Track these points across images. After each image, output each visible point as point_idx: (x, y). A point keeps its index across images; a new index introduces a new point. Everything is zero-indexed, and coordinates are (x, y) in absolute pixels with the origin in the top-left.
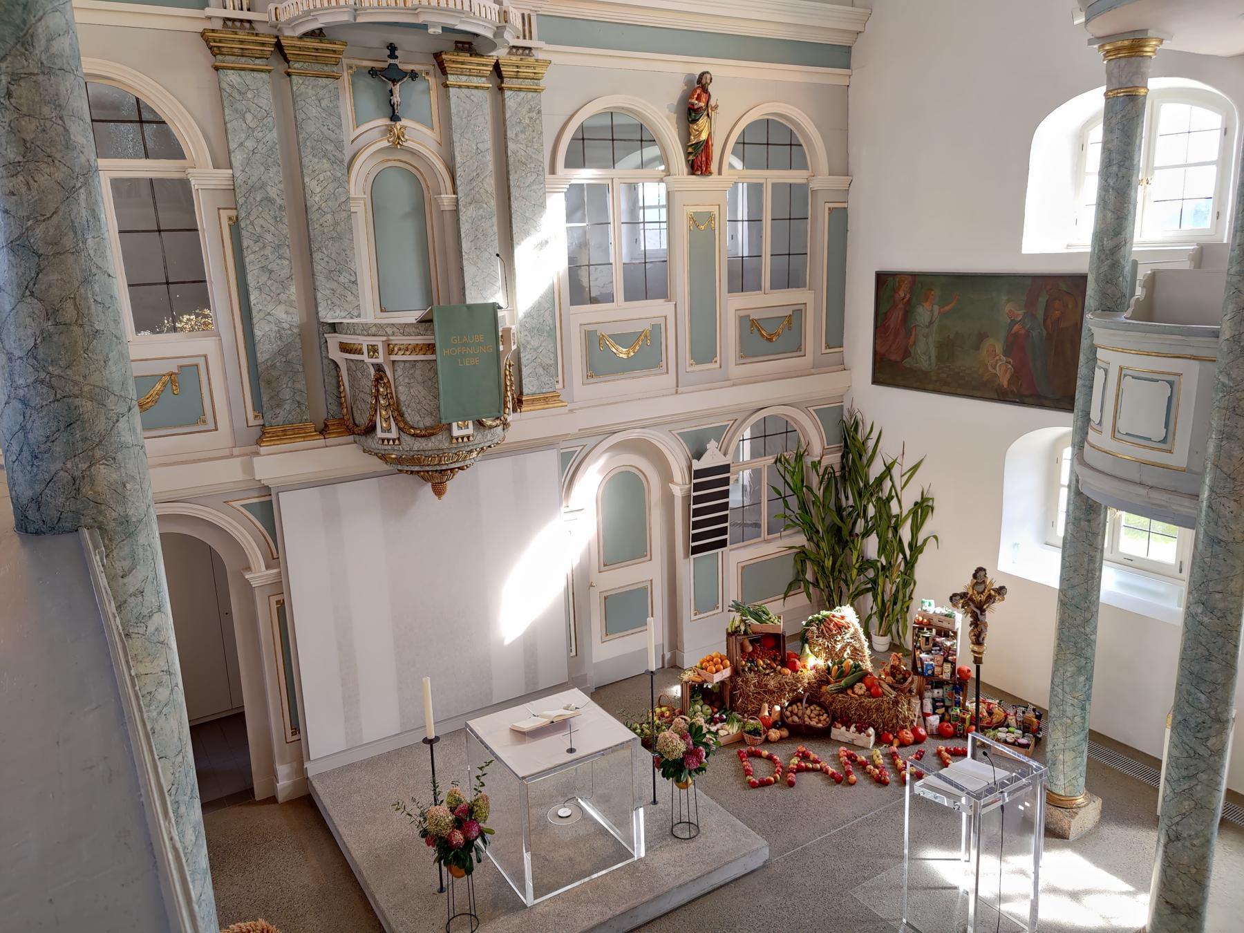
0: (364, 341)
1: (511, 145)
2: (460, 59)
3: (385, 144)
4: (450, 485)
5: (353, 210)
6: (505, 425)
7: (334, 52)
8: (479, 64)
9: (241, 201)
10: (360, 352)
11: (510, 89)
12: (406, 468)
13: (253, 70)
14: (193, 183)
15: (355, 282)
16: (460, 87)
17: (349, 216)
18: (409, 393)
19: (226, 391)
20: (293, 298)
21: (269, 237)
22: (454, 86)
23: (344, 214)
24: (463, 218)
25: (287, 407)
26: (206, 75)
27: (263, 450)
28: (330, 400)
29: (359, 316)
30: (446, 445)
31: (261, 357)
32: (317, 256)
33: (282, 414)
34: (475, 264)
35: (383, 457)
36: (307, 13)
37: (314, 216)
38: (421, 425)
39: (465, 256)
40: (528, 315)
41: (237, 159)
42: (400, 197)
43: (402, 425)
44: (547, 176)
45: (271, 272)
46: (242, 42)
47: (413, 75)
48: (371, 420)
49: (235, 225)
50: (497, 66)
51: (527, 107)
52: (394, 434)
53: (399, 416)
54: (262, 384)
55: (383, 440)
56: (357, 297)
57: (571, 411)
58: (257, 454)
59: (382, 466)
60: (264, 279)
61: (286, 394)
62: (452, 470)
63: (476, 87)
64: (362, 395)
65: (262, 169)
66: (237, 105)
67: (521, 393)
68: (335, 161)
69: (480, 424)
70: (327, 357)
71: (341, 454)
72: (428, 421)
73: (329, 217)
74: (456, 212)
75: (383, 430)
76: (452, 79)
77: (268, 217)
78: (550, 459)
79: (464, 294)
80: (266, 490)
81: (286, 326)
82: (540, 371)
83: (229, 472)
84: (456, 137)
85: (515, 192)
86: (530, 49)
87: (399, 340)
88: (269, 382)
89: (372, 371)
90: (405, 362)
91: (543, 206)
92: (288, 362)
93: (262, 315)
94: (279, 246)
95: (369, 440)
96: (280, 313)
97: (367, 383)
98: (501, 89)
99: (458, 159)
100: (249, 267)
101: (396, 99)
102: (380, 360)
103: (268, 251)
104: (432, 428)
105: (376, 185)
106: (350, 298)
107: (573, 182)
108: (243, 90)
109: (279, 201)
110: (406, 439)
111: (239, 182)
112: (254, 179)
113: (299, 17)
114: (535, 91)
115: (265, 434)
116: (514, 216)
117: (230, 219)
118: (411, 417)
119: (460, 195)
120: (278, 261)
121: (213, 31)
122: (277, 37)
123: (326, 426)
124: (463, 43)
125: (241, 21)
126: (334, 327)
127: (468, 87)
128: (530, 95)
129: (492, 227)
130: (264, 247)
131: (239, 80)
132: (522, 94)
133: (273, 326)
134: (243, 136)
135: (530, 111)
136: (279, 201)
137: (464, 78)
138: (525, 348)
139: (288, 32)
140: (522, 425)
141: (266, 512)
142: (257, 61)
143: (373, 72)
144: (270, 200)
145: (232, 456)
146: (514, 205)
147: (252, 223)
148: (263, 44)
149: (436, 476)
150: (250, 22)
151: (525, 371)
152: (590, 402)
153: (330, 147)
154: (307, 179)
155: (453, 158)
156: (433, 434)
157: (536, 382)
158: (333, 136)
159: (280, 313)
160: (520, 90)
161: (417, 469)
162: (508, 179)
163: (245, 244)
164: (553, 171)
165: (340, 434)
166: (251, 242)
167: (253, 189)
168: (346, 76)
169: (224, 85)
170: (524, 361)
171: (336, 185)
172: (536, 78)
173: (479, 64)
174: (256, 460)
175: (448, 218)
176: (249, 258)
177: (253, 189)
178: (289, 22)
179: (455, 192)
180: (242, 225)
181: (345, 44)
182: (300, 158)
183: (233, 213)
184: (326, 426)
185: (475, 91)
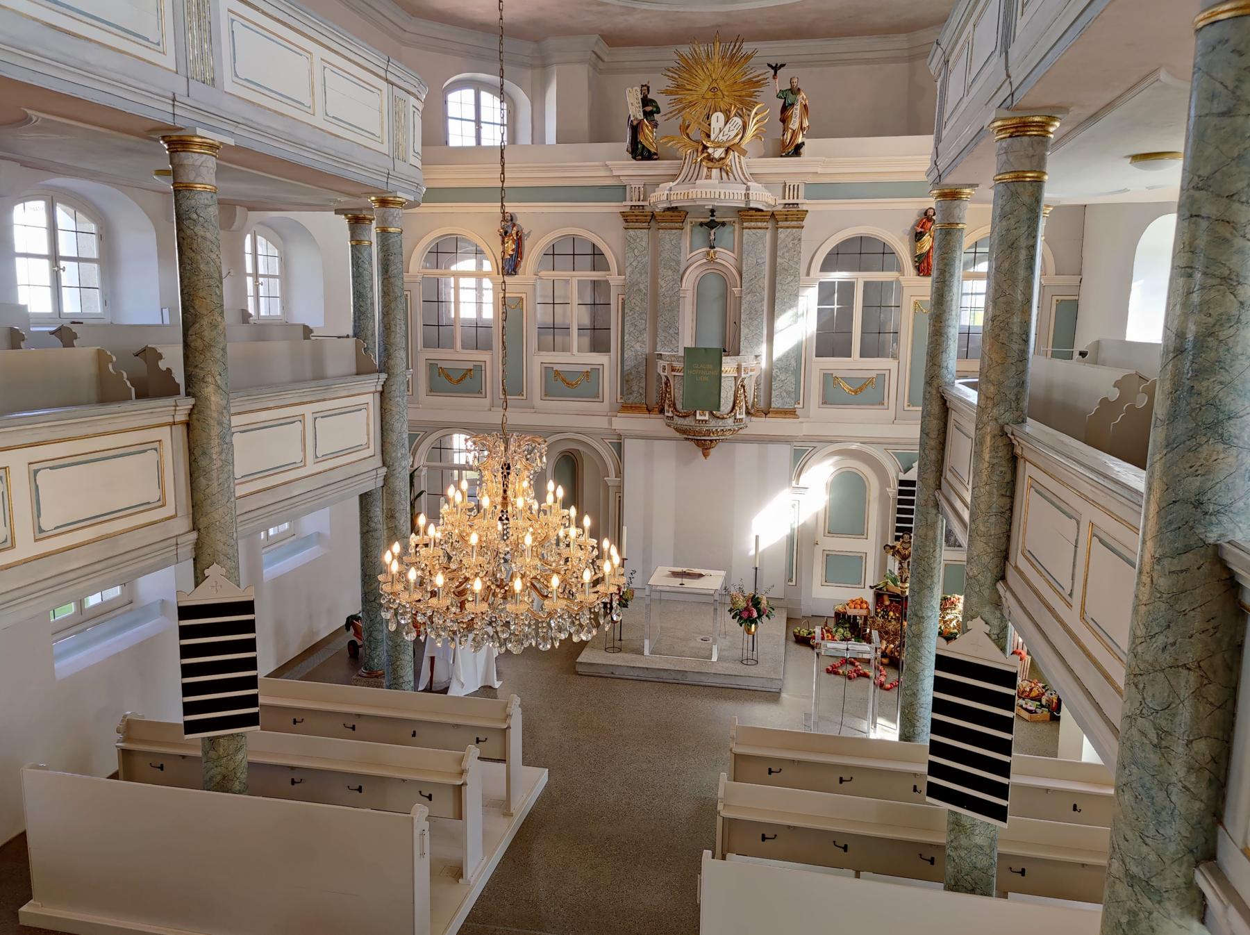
19: (609, 384)
26: (621, 231)
41: (628, 271)
42: (714, 288)
44: (803, 277)
47: (723, 224)
49: (623, 304)
61: (635, 388)
68: (676, 271)
85: (778, 287)
91: (797, 296)
96: (637, 346)
101: (712, 237)
141: (619, 448)
143: (701, 224)
144: (640, 290)
152: (816, 418)
159: (637, 346)
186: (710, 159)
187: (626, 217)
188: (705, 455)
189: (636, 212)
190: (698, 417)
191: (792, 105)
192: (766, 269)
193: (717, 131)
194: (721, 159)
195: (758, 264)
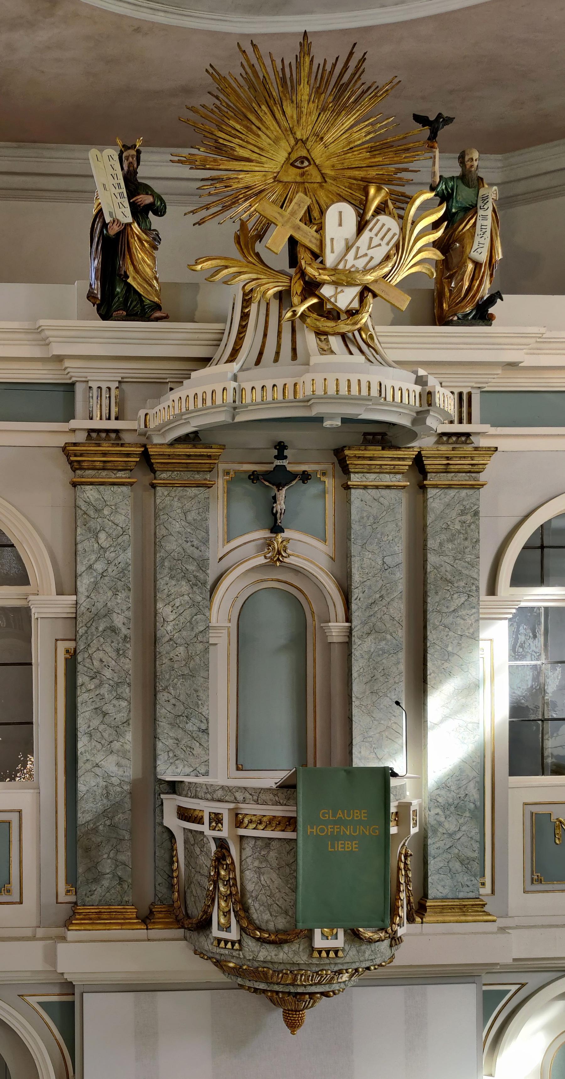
0: (206, 808)
1: (432, 559)
2: (368, 453)
3: (261, 560)
4: (308, 1015)
5: (211, 641)
6: (395, 940)
7: (209, 457)
8: (393, 459)
9: (81, 631)
10: (199, 821)
11: (436, 486)
12: (248, 984)
13: (113, 484)
14: (33, 611)
15: (205, 731)
16: (365, 487)
17: (206, 650)
18: (257, 878)
19: (38, 858)
20: (128, 747)
21: (108, 673)
22: (357, 487)
23: (200, 647)
24: (356, 653)
25: (106, 883)
27: (71, 935)
28: (159, 880)
29: (206, 774)
30: (303, 958)
31: (83, 818)
32: (162, 697)
33: (99, 891)
34: (369, 713)
35: (219, 964)
36: (179, 417)
37: (163, 648)
38: (271, 926)
39: (355, 703)
40: (443, 786)
41: (84, 583)
42: (275, 625)
43: (245, 924)
44: (483, 597)
45: (105, 714)
46: (104, 454)
47: (305, 477)
48: (205, 912)
50: (418, 460)
51: (459, 508)
52: (234, 935)
53: (242, 909)
54: (80, 852)
55: (219, 940)
56: (207, 749)
57: (502, 930)
58: (63, 939)
59: (217, 976)
60: (95, 723)
61: (107, 866)
62: (312, 995)
63: (388, 487)
64: (198, 877)
65: (110, 594)
66: (92, 524)
67: (425, 896)
68: (196, 583)
69: (354, 935)
70: (161, 824)
71: (166, 953)
72: (281, 923)
73: (181, 649)
74: (348, 645)
75: (220, 928)
76: (355, 479)
77: (109, 649)
78: (465, 998)
79: (351, 753)
80: (68, 987)
81: (115, 781)
82: (457, 866)
83: (26, 959)
84: (355, 549)
85: (433, 618)
86: (468, 435)
87: (251, 809)
88: (87, 850)
89: (213, 847)
90: (256, 838)
91: (474, 637)
92: (113, 827)
93: (88, 766)
94: (118, 684)
95: (202, 939)
97: (205, 863)
98: (423, 488)
99: (356, 577)
100: (81, 709)
101: (280, 506)
102: (224, 834)
103: (104, 690)
104: (285, 932)
105: (246, 611)
106: (198, 750)
107: (523, 604)
108: (99, 507)
109: (124, 631)
110: (250, 944)
111: (82, 609)
112: (99, 605)
113: (170, 422)
114: (472, 487)
115: (75, 916)
116: (430, 651)
117: (67, 651)
118: (259, 914)
119: (356, 622)
120: (114, 702)
121: (75, 444)
122: (144, 446)
123: (151, 912)
124: (374, 434)
125: (107, 431)
126: (174, 787)
127: (377, 487)
128: (464, 493)
129: (399, 665)
130: (101, 685)
131: (96, 495)
132: (452, 493)
133: (100, 780)
134: (93, 557)
135: (463, 513)
136: (124, 631)
137: (372, 476)
138: (435, 831)
139: (157, 440)
140: (421, 942)
142: (120, 474)
143: (254, 477)
144: (113, 630)
145: (34, 938)
146: (432, 636)
147: (90, 657)
148: (128, 455)
149: (291, 999)
150: (117, 431)
151: (433, 865)
153: (192, 567)
154: (160, 605)
155: (348, 576)
156: (286, 942)
157: (448, 882)
158: (196, 553)
159: (110, 764)
160: (450, 487)
161: (262, 986)
162: (425, 602)
163: (80, 681)
164: (492, 590)
165: (167, 926)
166: (86, 679)
167: (97, 617)
168: (221, 483)
169: (81, 503)
170: (432, 850)
171: (194, 611)
172: (475, 470)
173: (393, 459)
174: (61, 947)
175: (336, 653)
176: (82, 697)
177: (97, 617)
178: (158, 429)
179: (348, 620)
180: (80, 658)
181: (223, 447)
182: (155, 581)
183: (71, 645)
184: (151, 912)
185: (385, 492)
186: (324, 310)
187: (73, 457)
188: (293, 1023)
189: (105, 447)
190: (319, 942)
191: (471, 209)
192: (400, 578)
193: (340, 246)
194: (351, 313)
195: (385, 567)
